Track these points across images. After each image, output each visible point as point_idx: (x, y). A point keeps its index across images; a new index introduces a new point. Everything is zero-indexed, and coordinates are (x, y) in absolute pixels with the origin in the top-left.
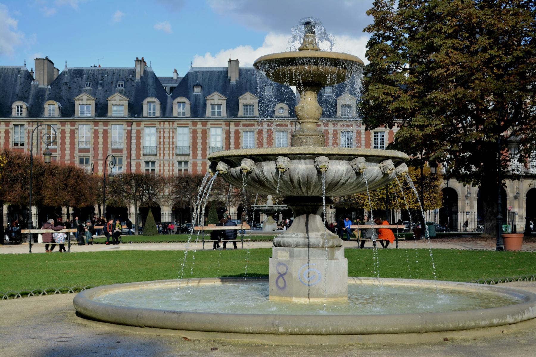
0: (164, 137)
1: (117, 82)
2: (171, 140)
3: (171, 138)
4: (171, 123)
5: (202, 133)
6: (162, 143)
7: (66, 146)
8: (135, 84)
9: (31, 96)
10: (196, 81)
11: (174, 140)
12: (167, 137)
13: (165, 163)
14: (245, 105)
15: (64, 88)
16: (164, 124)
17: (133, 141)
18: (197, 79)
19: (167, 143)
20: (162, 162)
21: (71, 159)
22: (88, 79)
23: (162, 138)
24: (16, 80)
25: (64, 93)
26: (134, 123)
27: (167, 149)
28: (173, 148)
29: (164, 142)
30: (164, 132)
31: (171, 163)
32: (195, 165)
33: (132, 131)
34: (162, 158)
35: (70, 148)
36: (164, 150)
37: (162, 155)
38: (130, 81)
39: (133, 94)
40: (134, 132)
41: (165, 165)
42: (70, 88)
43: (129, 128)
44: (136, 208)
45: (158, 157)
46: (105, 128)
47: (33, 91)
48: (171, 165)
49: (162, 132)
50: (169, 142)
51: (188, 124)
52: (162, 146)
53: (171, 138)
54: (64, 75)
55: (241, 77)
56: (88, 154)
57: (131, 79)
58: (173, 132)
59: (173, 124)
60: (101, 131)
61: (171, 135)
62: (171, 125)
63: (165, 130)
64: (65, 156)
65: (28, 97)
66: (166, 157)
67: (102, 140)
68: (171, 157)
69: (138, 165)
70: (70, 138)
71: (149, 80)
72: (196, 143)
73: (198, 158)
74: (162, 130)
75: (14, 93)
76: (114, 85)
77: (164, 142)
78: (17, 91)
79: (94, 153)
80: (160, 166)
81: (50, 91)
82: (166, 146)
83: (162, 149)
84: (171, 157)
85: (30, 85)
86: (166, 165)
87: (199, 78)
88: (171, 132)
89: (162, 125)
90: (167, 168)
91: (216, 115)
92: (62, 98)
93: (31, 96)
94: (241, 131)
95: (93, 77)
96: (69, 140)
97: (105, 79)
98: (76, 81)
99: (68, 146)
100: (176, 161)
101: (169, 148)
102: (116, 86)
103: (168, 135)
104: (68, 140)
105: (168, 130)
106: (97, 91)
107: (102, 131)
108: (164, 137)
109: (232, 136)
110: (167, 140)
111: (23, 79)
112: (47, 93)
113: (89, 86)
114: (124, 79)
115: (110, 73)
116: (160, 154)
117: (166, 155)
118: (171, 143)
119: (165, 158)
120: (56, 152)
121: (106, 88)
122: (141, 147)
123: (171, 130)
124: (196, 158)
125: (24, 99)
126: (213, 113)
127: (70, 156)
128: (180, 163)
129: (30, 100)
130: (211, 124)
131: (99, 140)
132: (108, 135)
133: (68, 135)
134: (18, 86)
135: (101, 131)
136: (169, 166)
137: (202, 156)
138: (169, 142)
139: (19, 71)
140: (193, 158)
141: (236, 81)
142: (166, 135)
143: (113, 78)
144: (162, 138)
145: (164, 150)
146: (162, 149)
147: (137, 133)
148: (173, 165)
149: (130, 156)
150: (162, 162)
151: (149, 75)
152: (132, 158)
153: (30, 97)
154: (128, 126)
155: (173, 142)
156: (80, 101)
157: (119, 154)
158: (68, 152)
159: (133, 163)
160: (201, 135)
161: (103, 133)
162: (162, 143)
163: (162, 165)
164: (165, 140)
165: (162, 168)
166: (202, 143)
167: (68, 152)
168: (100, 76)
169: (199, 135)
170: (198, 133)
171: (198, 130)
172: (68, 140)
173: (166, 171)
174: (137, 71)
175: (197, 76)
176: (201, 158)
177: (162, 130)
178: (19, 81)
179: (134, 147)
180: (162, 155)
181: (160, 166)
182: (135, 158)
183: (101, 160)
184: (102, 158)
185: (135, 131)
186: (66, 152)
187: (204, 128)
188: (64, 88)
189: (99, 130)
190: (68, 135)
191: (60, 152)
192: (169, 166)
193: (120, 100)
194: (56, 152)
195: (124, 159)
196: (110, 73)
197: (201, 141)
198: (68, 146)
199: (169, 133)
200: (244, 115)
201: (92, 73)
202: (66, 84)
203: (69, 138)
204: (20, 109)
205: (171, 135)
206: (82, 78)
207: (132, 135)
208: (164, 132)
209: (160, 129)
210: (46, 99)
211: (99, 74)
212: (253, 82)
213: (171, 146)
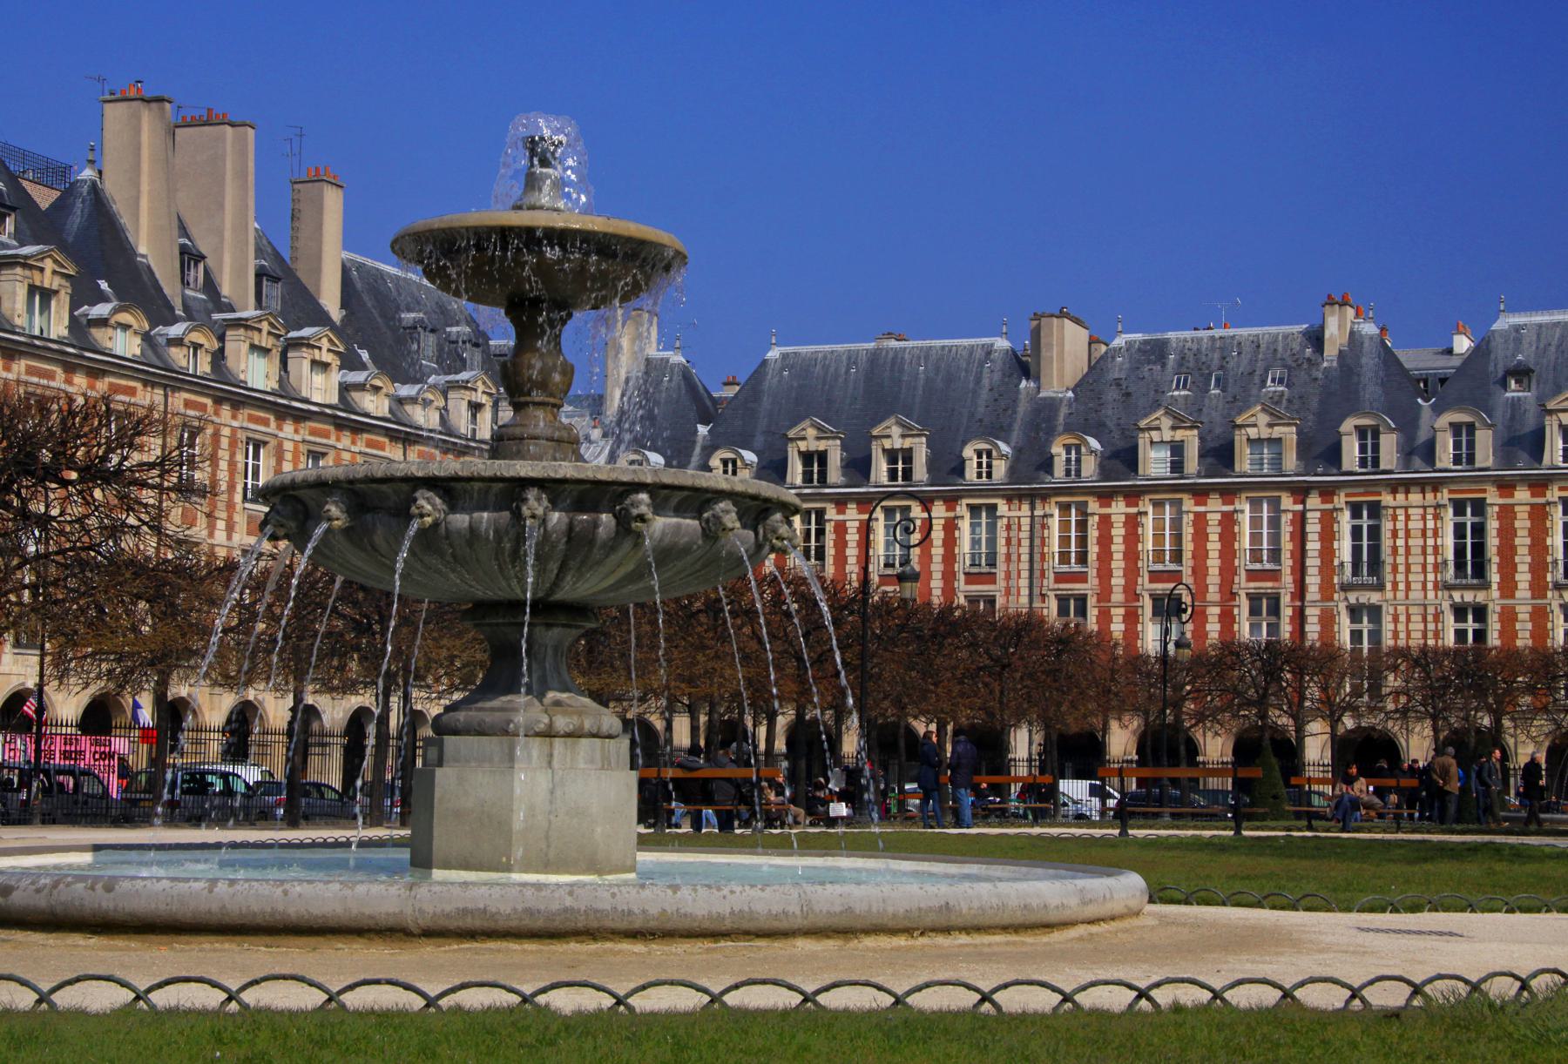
0: (1407, 532)
1: (1266, 371)
2: (1430, 542)
3: (1430, 533)
4: (1428, 489)
5: (1531, 516)
6: (1401, 551)
7: (1114, 565)
8: (1320, 376)
9: (1019, 422)
10: (1514, 356)
11: (1439, 542)
12: (1416, 533)
13: (1412, 610)
14: (1255, 443)
15: (1112, 394)
17: (1309, 546)
18: (1517, 350)
19: (1416, 550)
20: (1401, 609)
21: (1127, 600)
22: (1181, 365)
23: (1401, 534)
24: (978, 380)
25: (1111, 414)
27: (1416, 568)
28: (1436, 566)
29: (1408, 548)
30: (1408, 517)
31: (1431, 610)
32: (1508, 617)
33: (1309, 515)
34: (1401, 595)
35: (1125, 570)
36: (1408, 571)
37: (1402, 586)
38: (1305, 366)
39: (1314, 403)
40: (1313, 518)
41: (1413, 618)
42: (1128, 395)
43: (1299, 507)
44: (694, 729)
45: (1389, 595)
46: (841, 517)
47: (1023, 408)
48: (1430, 618)
49: (1401, 518)
50: (1424, 548)
52: (1401, 560)
53: (1430, 533)
54: (1113, 358)
56: (991, 587)
57: (1309, 360)
58: (1436, 517)
61: (1430, 524)
63: (1411, 511)
64: (1110, 592)
65: (1010, 425)
66: (1416, 595)
67: (1218, 546)
68: (1431, 595)
69: (1327, 620)
70: (1126, 539)
71: (1364, 360)
73: (1518, 594)
74: (1400, 512)
75: (972, 415)
76: (1257, 379)
77: (1408, 548)
78: (981, 410)
79: (1100, 584)
80: (1396, 620)
81: (1070, 406)
82: (1416, 559)
83: (1401, 568)
84: (1431, 595)
85: (1018, 392)
86: (1416, 618)
87: (1525, 345)
88: (1429, 517)
89: (1430, 496)
90: (1416, 625)
92: (1104, 425)
93: (1019, 422)
95: (1197, 361)
96: (1122, 548)
97: (1231, 364)
98: (1146, 374)
99: (1118, 563)
100: (1446, 605)
101: (1424, 566)
102: (1264, 382)
103: (1420, 525)
104: (1118, 547)
105: (1421, 511)
106: (1207, 401)
107: (1218, 516)
108: (1407, 532)
110: (1416, 542)
111: (997, 376)
112: (1064, 411)
113: (1184, 387)
114: (1289, 362)
115: (1247, 348)
116: (1395, 584)
117: (1416, 586)
118: (1430, 550)
119: (1412, 595)
120: (1086, 581)
121: (1232, 389)
122: (1336, 563)
124: (1513, 597)
125: (996, 429)
127: (1125, 591)
128: (1460, 612)
129: (1016, 434)
131: (1210, 546)
132: (1236, 529)
133: (1118, 532)
134: (984, 394)
136: (1425, 620)
137: (1532, 587)
138: (1424, 548)
139: (989, 353)
140: (1502, 597)
142: (1415, 525)
143: (1253, 361)
144: (1401, 534)
145: (1408, 571)
146: (1401, 568)
147: (1195, 523)
148: (1437, 617)
149: (1300, 590)
150: (1401, 609)
151: (1366, 345)
152: (1309, 597)
153: (1016, 427)
154: (1295, 503)
155: (1436, 547)
156: (1153, 433)
157: (1269, 584)
158: (1118, 580)
159: (1312, 614)
160: (1528, 524)
161: (1220, 523)
162: (1401, 551)
163: (1402, 618)
164: (1411, 542)
165: (1401, 627)
166: (1531, 547)
167: (1118, 580)
168: (1216, 356)
171: (1517, 509)
172: (1118, 547)
173: (1416, 635)
174: (1327, 335)
175: (1518, 341)
176: (1528, 594)
177: (1400, 512)
178: (986, 382)
179: (1313, 562)
180: (1402, 586)
181: (1396, 620)
182: (1318, 597)
183: (1214, 604)
184: (1217, 597)
185: (1318, 514)
186: (1114, 581)
188: (1112, 394)
189: (1209, 516)
190: (1118, 532)
191: (1096, 581)
192: (1425, 620)
193: (1271, 425)
194: (1086, 581)
195: (1286, 599)
196: (1247, 348)
197: (1528, 541)
198: (1118, 563)
199: (1424, 518)
201: (1195, 347)
202: (1119, 385)
203: (1120, 540)
204: (984, 460)
205: (1430, 524)
206: (1164, 365)
207: (1309, 528)
208: (1408, 517)
209: (1395, 508)
210: (1061, 428)
211: (1213, 349)
213: (1430, 559)
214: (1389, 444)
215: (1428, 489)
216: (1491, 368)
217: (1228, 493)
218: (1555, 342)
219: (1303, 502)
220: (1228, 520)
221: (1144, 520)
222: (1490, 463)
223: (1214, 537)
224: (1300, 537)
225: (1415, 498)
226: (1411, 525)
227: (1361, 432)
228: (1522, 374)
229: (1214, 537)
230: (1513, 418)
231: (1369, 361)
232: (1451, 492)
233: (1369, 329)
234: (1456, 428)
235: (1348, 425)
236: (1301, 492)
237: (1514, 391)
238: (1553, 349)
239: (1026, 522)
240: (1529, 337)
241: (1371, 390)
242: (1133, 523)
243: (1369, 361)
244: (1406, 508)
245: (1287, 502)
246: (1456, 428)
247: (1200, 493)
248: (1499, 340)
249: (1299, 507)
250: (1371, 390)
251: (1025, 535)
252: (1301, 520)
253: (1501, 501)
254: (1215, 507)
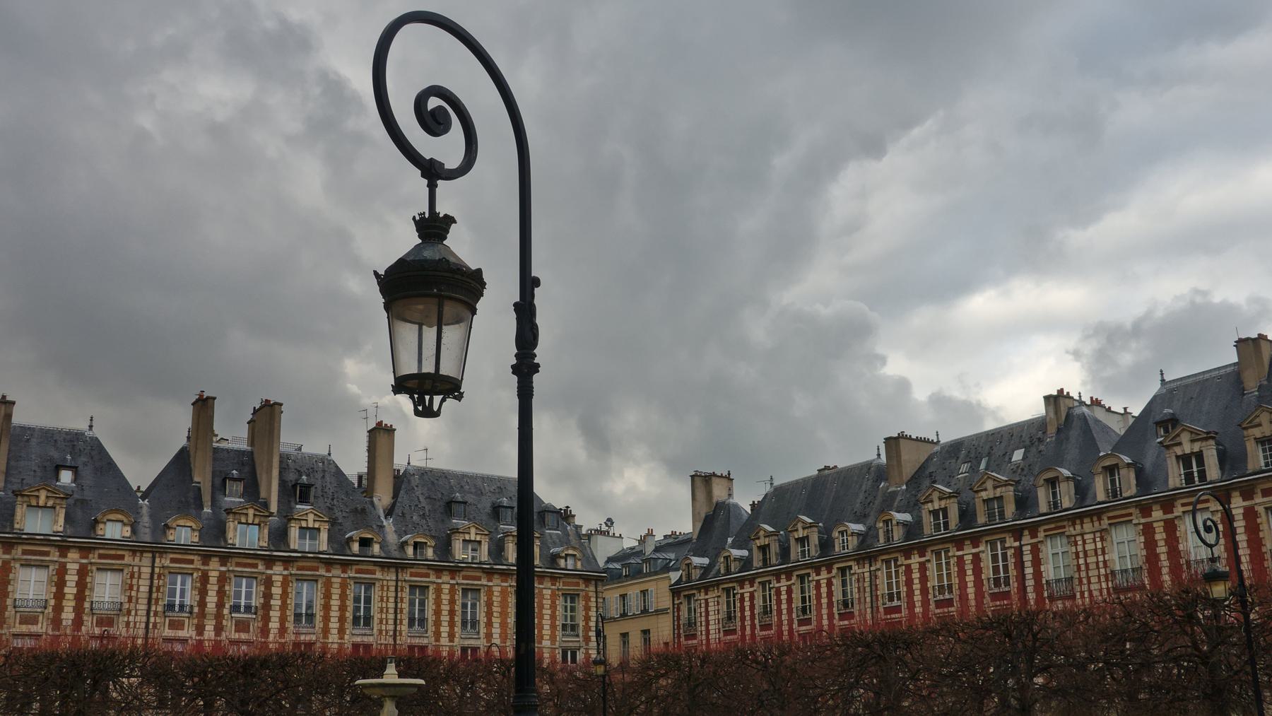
0: (1085, 552)
12: (1090, 553)
16: (1082, 524)
26: (1026, 532)
29: (1087, 564)
30: (1084, 542)
33: (1024, 548)
40: (1027, 549)
43: (1017, 544)
51: (1130, 514)
58: (1102, 539)
59: (1100, 519)
60: (968, 558)
62: (1096, 524)
63: (1086, 537)
72: (1157, 556)
74: (1079, 538)
77: (1087, 564)
82: (1092, 573)
94: (1261, 509)
105: (1091, 536)
109: (1240, 524)
110: (1091, 560)
112: (899, 498)
123: (1098, 535)
130: (1183, 505)
135: (968, 558)
155: (1105, 562)
169: (1160, 536)
170: (1157, 530)
171: (1155, 525)
177: (1079, 538)
187: (1170, 516)
199: (1095, 541)
205: (1099, 545)
208: (1084, 542)
213: (1102, 571)
215: (1095, 518)
217: (975, 540)
219: (1020, 540)
220: (976, 559)
221: (879, 573)
222: (1134, 490)
223: (969, 572)
224: (1020, 565)
225: (1088, 526)
226: (1088, 547)
229: (969, 572)
232: (1109, 518)
236: (1017, 533)
239: (867, 575)
242: (923, 568)
244: (1082, 535)
245: (1010, 542)
247: (959, 542)
249: (1017, 544)
251: (867, 584)
252: (1019, 552)
253: (1143, 521)
254: (968, 552)
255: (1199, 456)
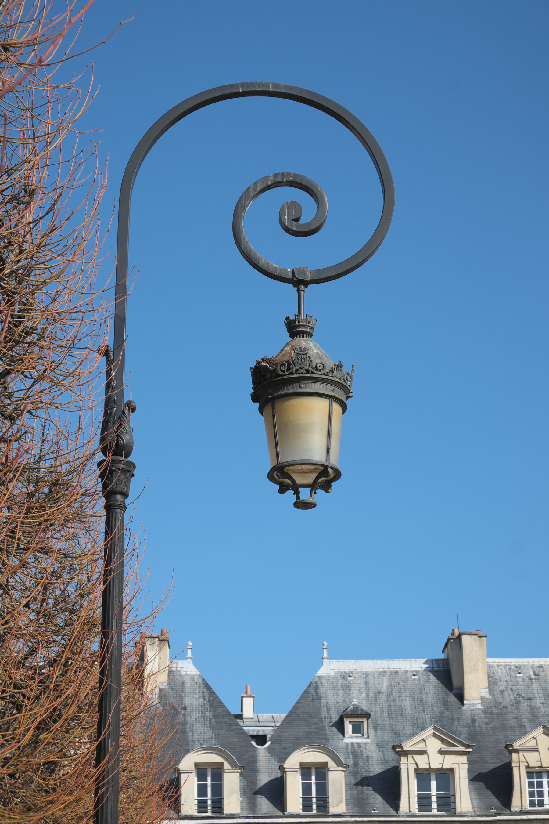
55: (497, 689)
91: (434, 806)
126: (424, 802)
141: (482, 698)
200: (532, 804)
212: (537, 702)
214: (232, 781)
216: (324, 713)
218: (384, 690)
227: (201, 770)
228: (359, 716)
230: (356, 764)
231: (193, 701)
233: (187, 668)
234: (305, 769)
235: (187, 763)
237: (350, 737)
238: (384, 697)
240: (357, 685)
241: (200, 730)
243: (193, 701)
246: (305, 769)
248: (326, 685)
250: (200, 730)
255: (445, 777)
